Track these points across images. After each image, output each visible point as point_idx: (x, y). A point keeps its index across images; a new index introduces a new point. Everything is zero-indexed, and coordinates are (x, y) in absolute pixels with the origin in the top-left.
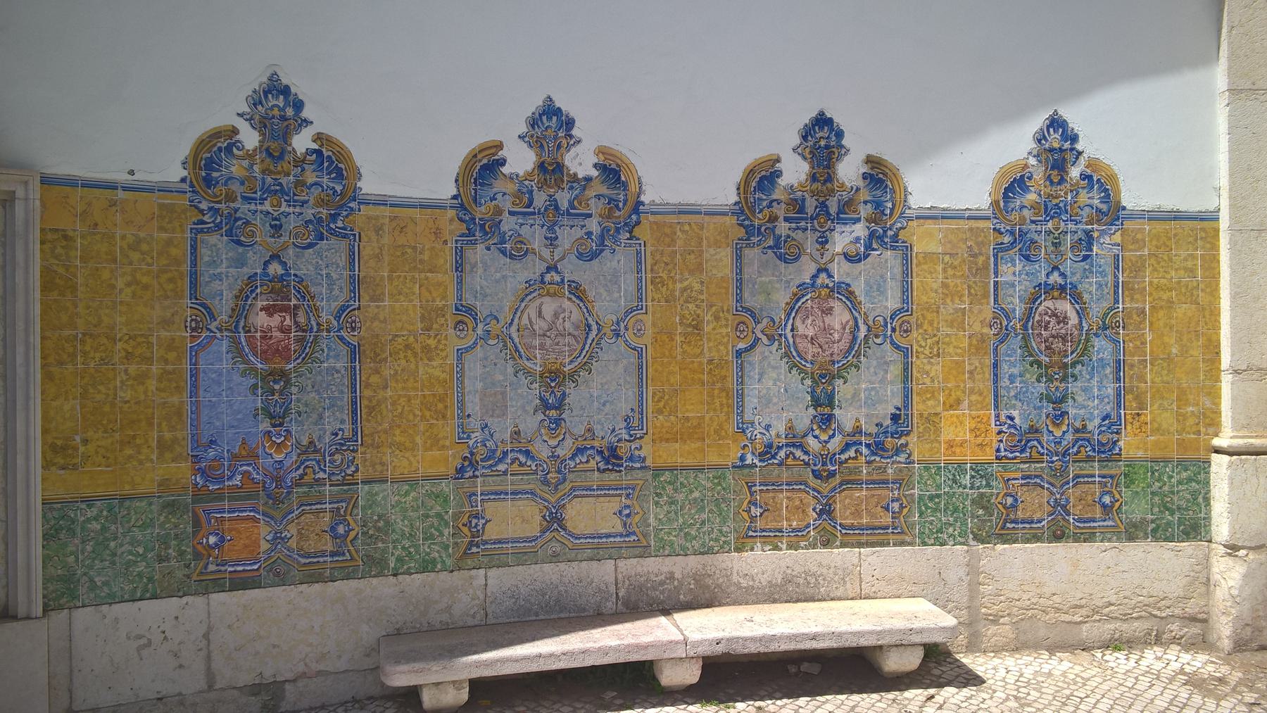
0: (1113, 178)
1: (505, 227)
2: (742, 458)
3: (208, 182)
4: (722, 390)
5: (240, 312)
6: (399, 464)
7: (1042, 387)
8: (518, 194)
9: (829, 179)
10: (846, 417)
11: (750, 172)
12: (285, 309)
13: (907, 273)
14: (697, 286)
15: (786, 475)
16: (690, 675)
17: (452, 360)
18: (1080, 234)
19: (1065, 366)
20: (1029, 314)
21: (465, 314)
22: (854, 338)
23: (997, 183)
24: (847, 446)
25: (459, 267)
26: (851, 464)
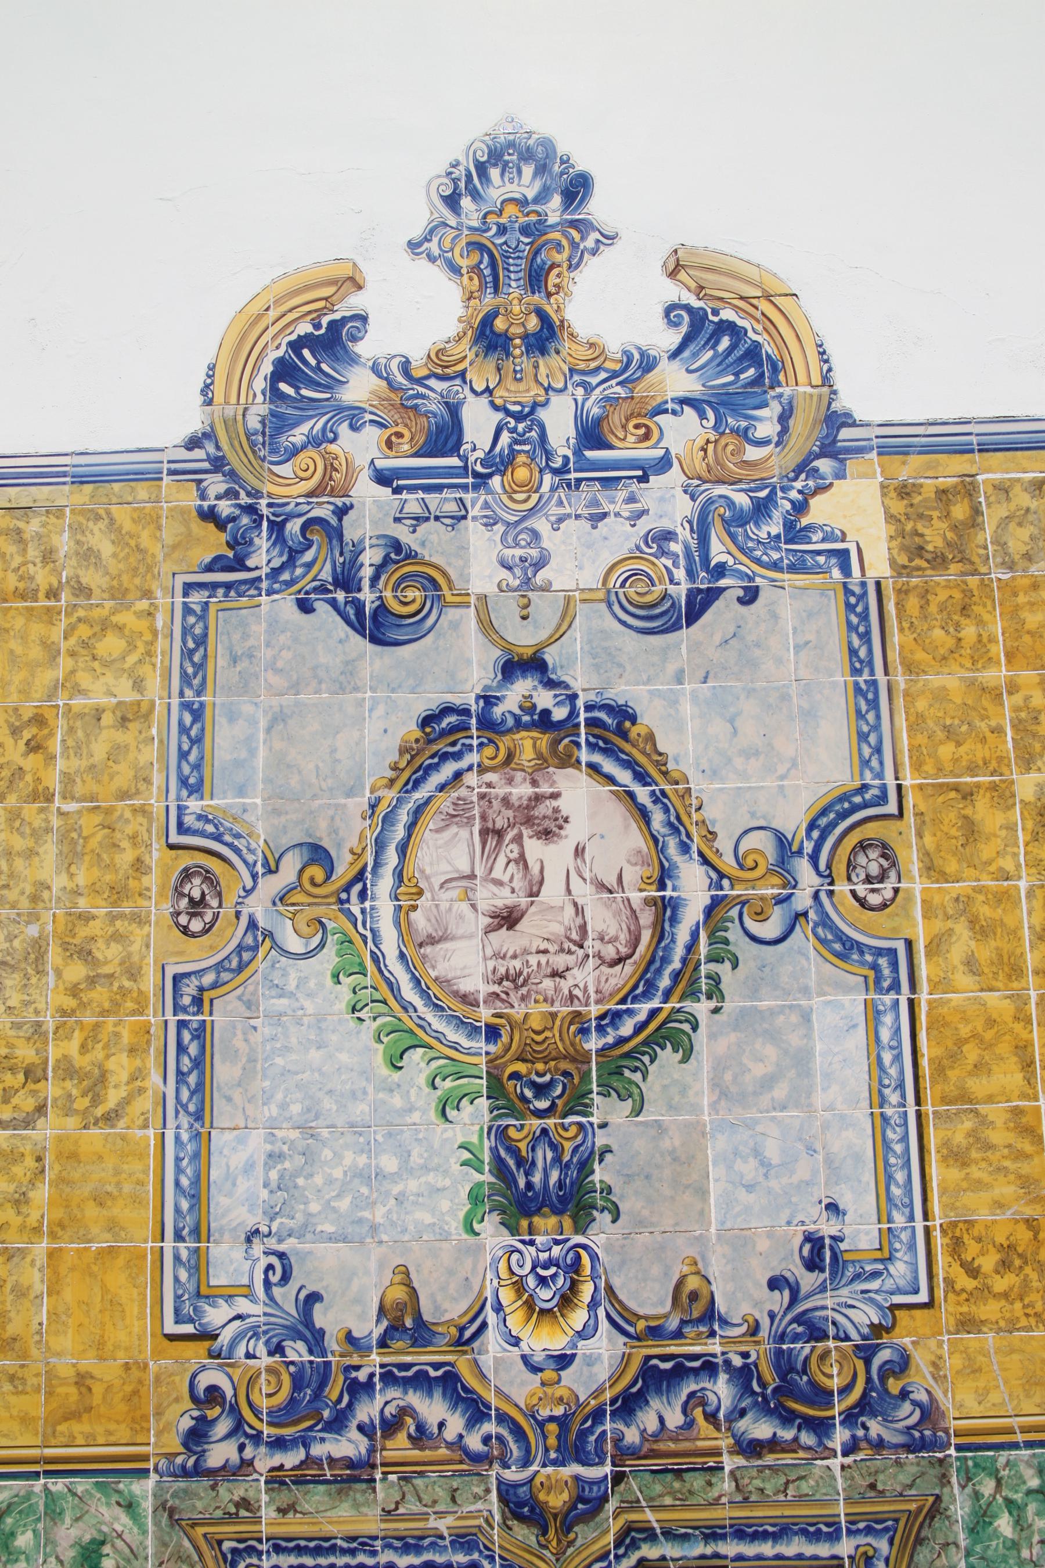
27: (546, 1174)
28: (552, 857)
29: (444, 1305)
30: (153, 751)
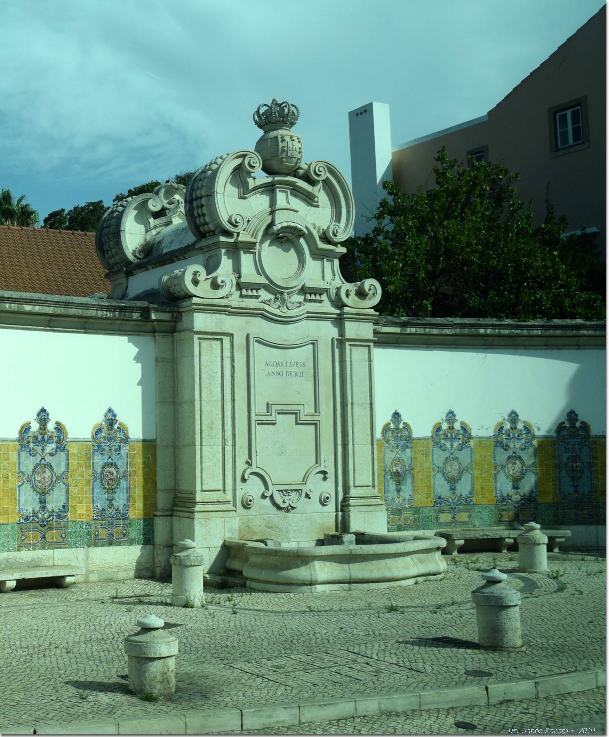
0: (126, 428)
2: (20, 521)
4: (14, 498)
9: (45, 429)
10: (50, 506)
11: (23, 427)
13: (68, 459)
14: (7, 465)
15: (32, 525)
16: (13, 584)
18: (117, 446)
19: (113, 489)
20: (102, 472)
22: (52, 481)
23: (94, 430)
24: (50, 516)
26: (51, 522)
27: (516, 486)
28: (516, 466)
29: (510, 495)
30: (492, 458)
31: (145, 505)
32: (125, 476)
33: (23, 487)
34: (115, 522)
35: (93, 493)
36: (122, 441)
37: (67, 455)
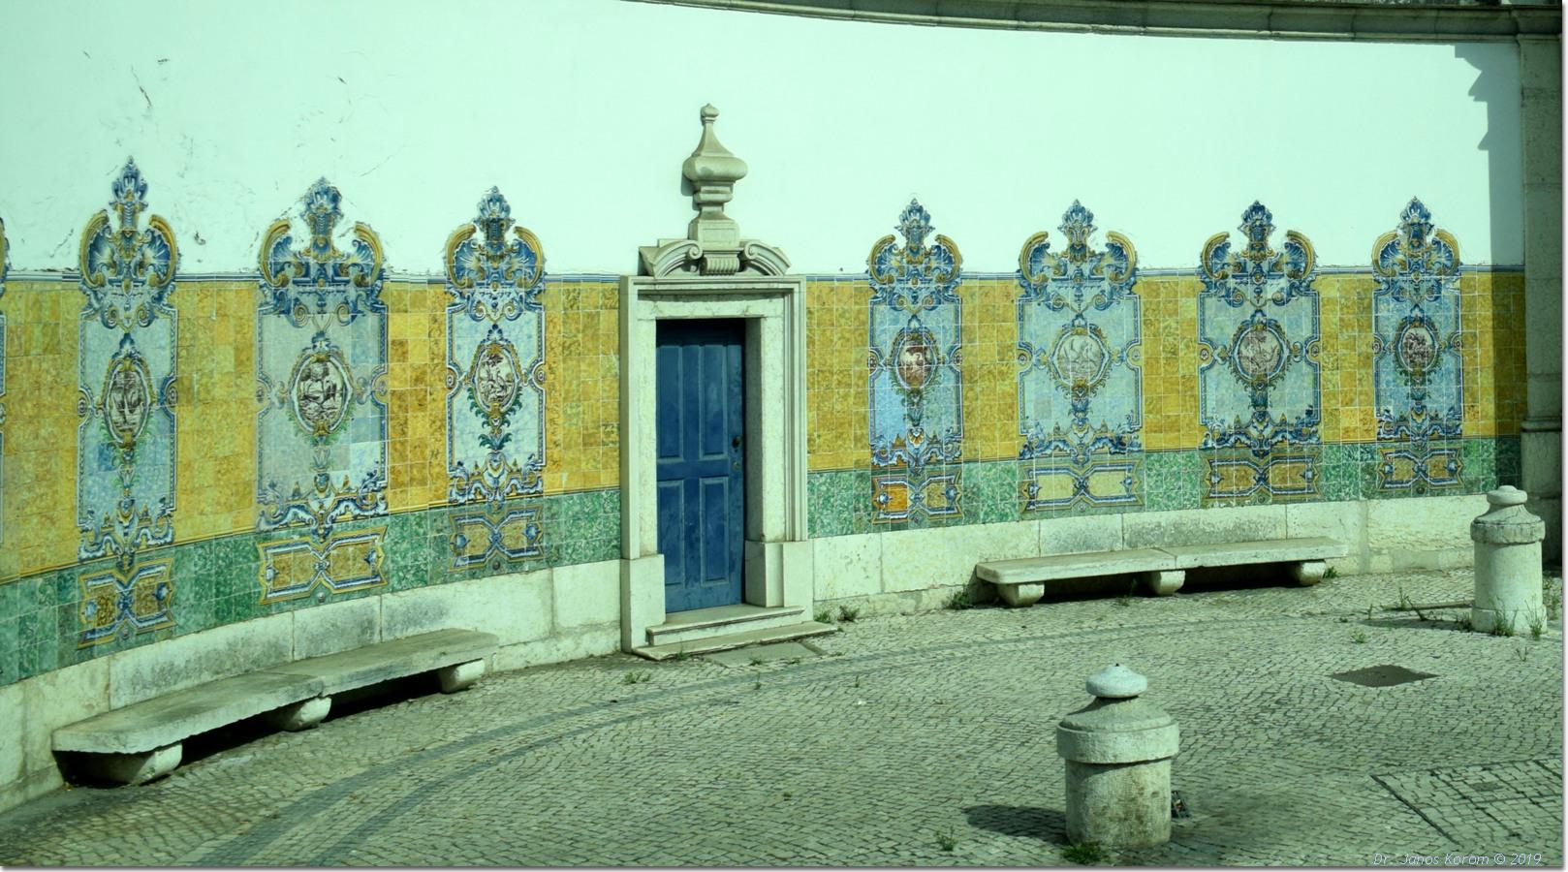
0: (1454, 243)
1: (1049, 290)
3: (879, 272)
5: (894, 353)
6: (984, 449)
7: (1408, 389)
8: (1058, 267)
9: (1263, 247)
10: (1276, 413)
11: (1210, 244)
12: (919, 350)
13: (1316, 311)
16: (1179, 579)
17: (1017, 379)
20: (1398, 339)
21: (1025, 350)
23: (1376, 250)
25: (1021, 318)
31: (1499, 407)
32: (1453, 345)
33: (1212, 373)
34: (1430, 445)
35: (1377, 383)
36: (1444, 270)
37: (1316, 304)
